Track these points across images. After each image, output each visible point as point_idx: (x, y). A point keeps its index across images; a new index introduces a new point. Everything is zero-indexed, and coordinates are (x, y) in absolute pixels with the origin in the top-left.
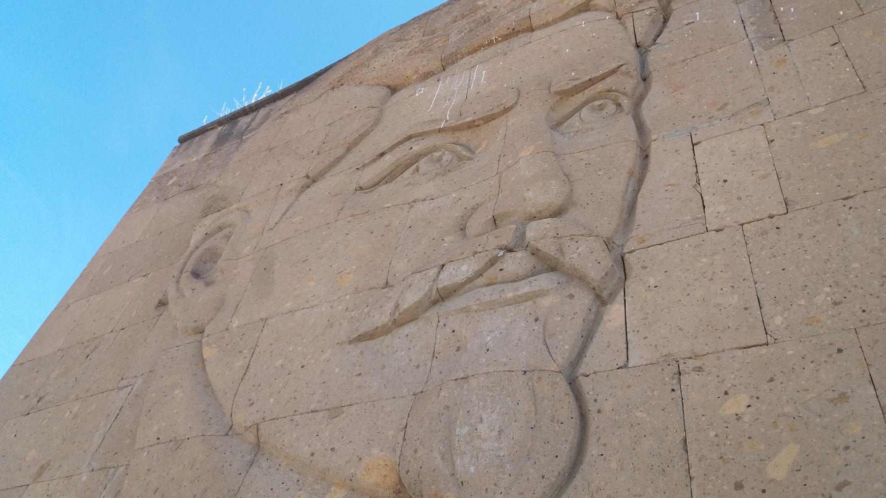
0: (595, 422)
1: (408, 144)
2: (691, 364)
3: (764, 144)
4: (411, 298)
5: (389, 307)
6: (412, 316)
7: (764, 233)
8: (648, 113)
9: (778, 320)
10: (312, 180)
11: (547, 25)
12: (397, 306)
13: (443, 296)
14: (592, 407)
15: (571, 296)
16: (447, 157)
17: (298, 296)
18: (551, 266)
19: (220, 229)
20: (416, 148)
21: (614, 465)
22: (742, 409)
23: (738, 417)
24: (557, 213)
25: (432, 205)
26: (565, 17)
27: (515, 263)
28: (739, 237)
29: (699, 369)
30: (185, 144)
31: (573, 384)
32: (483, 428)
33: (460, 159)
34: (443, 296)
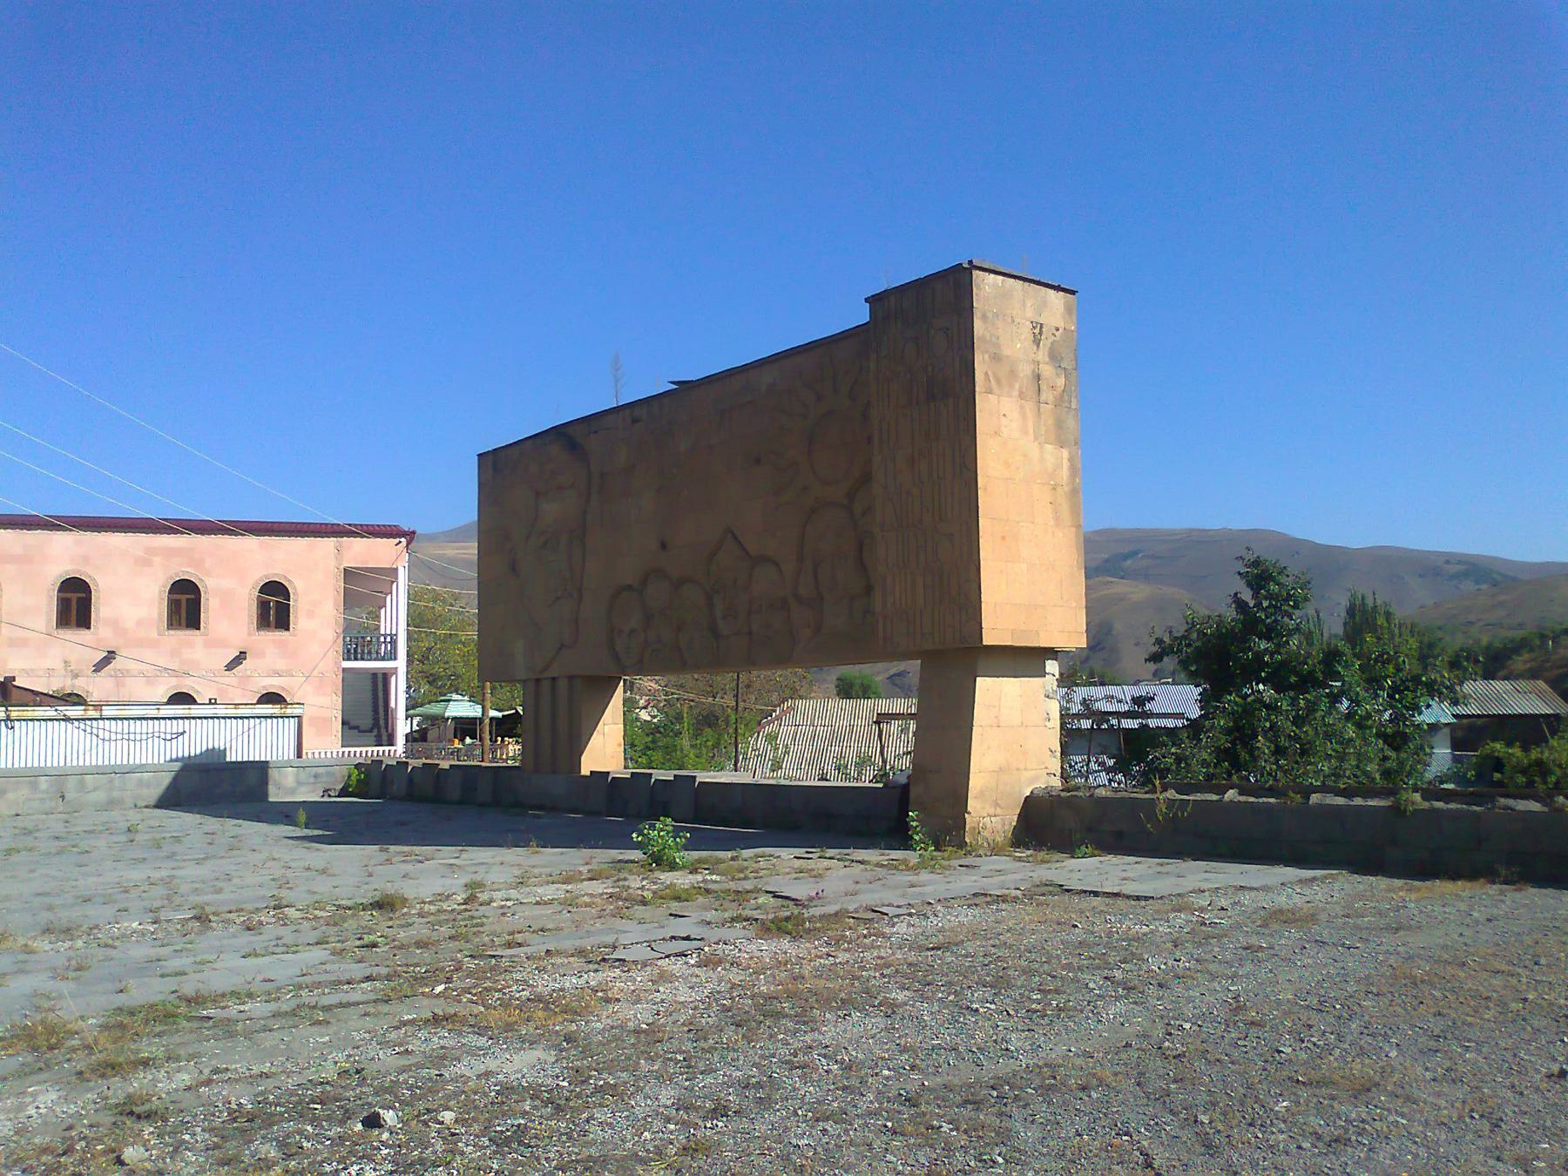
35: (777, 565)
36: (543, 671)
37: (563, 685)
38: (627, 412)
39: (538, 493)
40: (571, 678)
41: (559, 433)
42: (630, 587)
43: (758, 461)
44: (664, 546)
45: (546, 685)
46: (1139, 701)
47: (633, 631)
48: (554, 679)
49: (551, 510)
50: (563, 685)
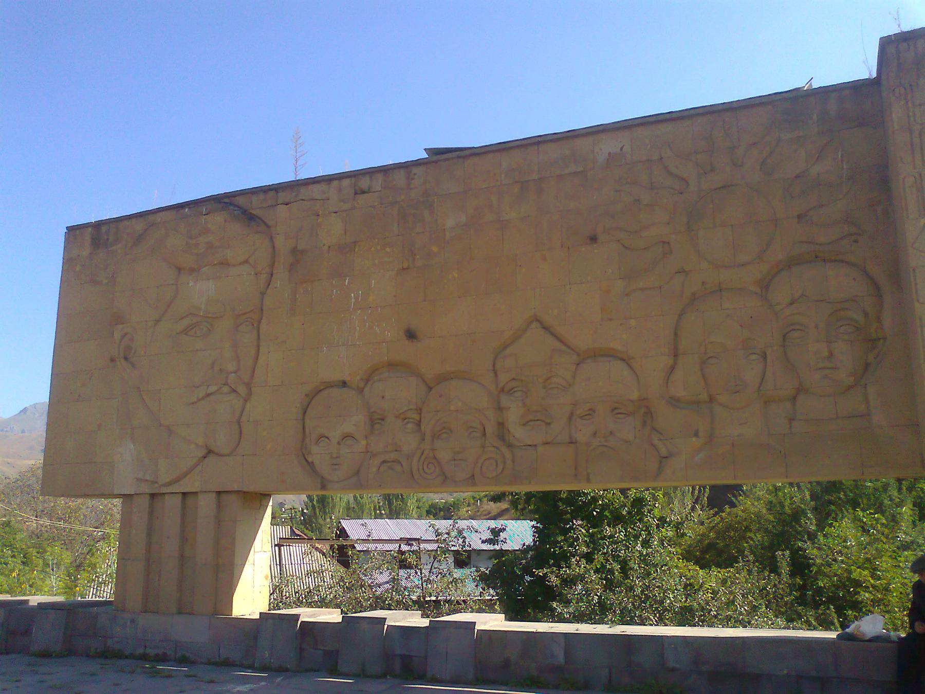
4: (201, 395)
6: (203, 398)
8: (261, 331)
10: (158, 321)
11: (234, 265)
13: (208, 395)
16: (205, 329)
18: (235, 391)
19: (126, 334)
20: (195, 321)
24: (235, 372)
26: (240, 264)
27: (226, 389)
34: (208, 395)
35: (626, 360)
36: (170, 484)
37: (206, 505)
38: (346, 182)
39: (179, 270)
40: (219, 493)
41: (223, 202)
42: (344, 384)
43: (593, 239)
44: (411, 335)
45: (172, 504)
46: (496, 532)
47: (347, 436)
48: (184, 494)
49: (202, 291)
50: (206, 505)
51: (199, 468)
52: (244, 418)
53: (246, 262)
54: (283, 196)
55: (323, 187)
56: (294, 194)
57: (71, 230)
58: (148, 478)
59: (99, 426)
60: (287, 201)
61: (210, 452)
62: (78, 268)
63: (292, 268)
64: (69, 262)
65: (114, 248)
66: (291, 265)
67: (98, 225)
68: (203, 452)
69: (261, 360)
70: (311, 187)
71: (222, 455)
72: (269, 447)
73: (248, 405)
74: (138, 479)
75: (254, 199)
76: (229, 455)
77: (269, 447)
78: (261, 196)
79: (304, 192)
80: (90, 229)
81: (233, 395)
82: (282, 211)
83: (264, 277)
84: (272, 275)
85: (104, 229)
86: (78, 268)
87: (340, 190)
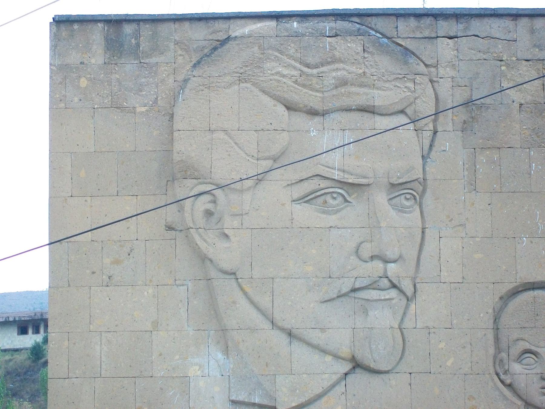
0: (408, 344)
1: (316, 180)
2: (433, 330)
3: (461, 248)
5: (336, 291)
7: (456, 289)
9: (455, 321)
12: (339, 291)
14: (407, 340)
15: (400, 300)
17: (286, 270)
18: (394, 286)
20: (322, 186)
21: (412, 357)
22: (443, 347)
23: (442, 349)
25: (340, 233)
28: (449, 288)
29: (434, 333)
30: (63, 27)
31: (400, 329)
32: (379, 346)
33: (346, 201)
51: (340, 389)
52: (408, 324)
53: (402, 112)
54: (444, 27)
55: (508, 23)
56: (461, 26)
57: (61, 22)
58: (257, 401)
59: (156, 324)
60: (452, 34)
61: (357, 365)
62: (84, 82)
63: (465, 127)
64: (62, 73)
65: (153, 60)
66: (465, 122)
67: (115, 22)
68: (347, 367)
69: (430, 246)
70: (486, 20)
71: (387, 372)
72: (449, 363)
73: (413, 306)
74: (234, 402)
75: (402, 24)
76: (387, 372)
77: (449, 363)
78: (412, 22)
79: (477, 26)
80: (100, 25)
81: (393, 293)
82: (445, 49)
83: (428, 135)
84: (435, 132)
85: (128, 29)
86: (84, 82)
87: (532, 31)
